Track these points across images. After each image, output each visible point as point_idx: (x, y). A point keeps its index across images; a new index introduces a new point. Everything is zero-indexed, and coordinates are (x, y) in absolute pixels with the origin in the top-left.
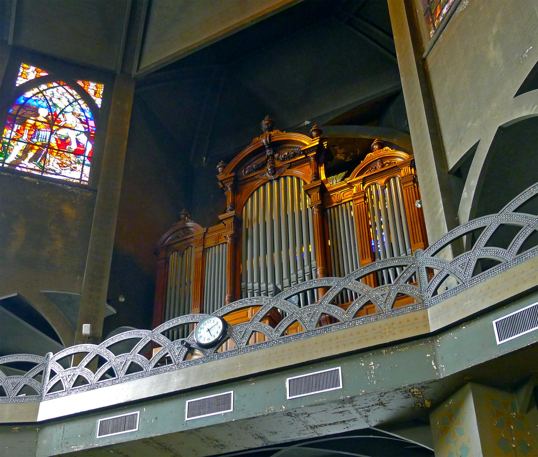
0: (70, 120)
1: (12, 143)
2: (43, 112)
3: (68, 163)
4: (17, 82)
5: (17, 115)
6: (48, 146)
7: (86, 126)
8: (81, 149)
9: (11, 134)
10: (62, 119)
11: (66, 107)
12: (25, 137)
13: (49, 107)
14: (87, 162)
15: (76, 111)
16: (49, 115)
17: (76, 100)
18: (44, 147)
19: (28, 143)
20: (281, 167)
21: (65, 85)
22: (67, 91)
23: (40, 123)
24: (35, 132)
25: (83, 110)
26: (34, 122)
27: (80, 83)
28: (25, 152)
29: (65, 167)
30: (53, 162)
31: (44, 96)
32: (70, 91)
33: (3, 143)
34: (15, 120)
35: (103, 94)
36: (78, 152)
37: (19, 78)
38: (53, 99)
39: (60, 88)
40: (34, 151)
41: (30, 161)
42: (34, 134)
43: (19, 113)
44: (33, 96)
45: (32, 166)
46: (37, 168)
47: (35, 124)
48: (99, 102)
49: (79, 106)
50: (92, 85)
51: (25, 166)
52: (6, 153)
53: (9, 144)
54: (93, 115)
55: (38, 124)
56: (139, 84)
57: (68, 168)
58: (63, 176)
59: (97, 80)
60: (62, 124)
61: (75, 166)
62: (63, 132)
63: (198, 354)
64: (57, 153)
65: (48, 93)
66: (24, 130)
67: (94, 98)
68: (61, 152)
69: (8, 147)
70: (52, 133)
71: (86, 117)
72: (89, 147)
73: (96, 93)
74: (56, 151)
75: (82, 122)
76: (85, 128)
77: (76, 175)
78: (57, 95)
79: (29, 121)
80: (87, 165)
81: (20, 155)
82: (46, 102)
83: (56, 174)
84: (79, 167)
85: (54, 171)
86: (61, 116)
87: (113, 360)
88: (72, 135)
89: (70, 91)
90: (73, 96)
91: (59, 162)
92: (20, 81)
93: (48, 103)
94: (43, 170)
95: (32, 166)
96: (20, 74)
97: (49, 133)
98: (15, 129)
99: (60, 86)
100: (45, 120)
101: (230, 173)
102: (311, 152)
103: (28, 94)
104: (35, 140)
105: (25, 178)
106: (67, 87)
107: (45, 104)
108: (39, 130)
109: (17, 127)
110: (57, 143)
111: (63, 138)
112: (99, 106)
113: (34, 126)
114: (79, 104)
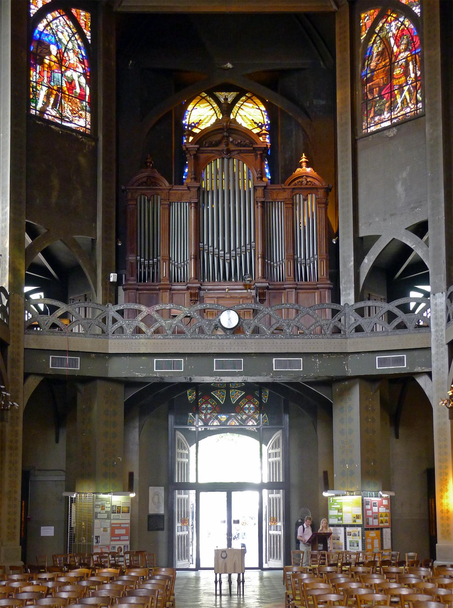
0: (72, 58)
1: (38, 87)
2: (53, 49)
3: (76, 109)
4: (31, 11)
6: (60, 90)
7: (83, 66)
8: (83, 93)
9: (36, 76)
10: (67, 59)
11: (68, 42)
12: (46, 80)
13: (56, 44)
14: (88, 108)
16: (57, 54)
18: (59, 92)
19: (49, 87)
20: (233, 151)
21: (64, 15)
22: (67, 23)
23: (53, 63)
24: (51, 73)
26: (49, 61)
27: (73, 11)
28: (48, 96)
29: (75, 114)
31: (52, 29)
32: (68, 22)
35: (91, 27)
36: (81, 97)
38: (58, 33)
39: (61, 18)
40: (54, 96)
41: (52, 109)
42: (51, 76)
43: (39, 51)
44: (44, 30)
45: (54, 113)
46: (58, 115)
47: (50, 63)
49: (75, 41)
50: (83, 13)
51: (50, 113)
52: (36, 100)
53: (36, 87)
55: (53, 63)
57: (77, 115)
58: (75, 124)
59: (84, 9)
60: (67, 64)
61: (81, 112)
63: (220, 332)
64: (69, 99)
65: (54, 26)
66: (44, 71)
68: (70, 97)
69: (36, 91)
70: (62, 74)
71: (82, 55)
73: (86, 25)
74: (67, 96)
75: (80, 62)
76: (83, 69)
77: (82, 123)
78: (60, 28)
82: (54, 37)
83: (71, 122)
84: (83, 113)
85: (68, 118)
86: (65, 55)
87: (164, 323)
88: (75, 76)
89: (68, 22)
90: (70, 29)
91: (71, 109)
92: (33, 10)
93: (55, 38)
94: (62, 118)
95: (54, 113)
97: (60, 75)
98: (38, 72)
99: (62, 16)
101: (195, 144)
102: (259, 150)
103: (41, 27)
104: (52, 83)
105: (52, 127)
107: (53, 40)
108: (54, 71)
111: (70, 81)
114: (76, 39)
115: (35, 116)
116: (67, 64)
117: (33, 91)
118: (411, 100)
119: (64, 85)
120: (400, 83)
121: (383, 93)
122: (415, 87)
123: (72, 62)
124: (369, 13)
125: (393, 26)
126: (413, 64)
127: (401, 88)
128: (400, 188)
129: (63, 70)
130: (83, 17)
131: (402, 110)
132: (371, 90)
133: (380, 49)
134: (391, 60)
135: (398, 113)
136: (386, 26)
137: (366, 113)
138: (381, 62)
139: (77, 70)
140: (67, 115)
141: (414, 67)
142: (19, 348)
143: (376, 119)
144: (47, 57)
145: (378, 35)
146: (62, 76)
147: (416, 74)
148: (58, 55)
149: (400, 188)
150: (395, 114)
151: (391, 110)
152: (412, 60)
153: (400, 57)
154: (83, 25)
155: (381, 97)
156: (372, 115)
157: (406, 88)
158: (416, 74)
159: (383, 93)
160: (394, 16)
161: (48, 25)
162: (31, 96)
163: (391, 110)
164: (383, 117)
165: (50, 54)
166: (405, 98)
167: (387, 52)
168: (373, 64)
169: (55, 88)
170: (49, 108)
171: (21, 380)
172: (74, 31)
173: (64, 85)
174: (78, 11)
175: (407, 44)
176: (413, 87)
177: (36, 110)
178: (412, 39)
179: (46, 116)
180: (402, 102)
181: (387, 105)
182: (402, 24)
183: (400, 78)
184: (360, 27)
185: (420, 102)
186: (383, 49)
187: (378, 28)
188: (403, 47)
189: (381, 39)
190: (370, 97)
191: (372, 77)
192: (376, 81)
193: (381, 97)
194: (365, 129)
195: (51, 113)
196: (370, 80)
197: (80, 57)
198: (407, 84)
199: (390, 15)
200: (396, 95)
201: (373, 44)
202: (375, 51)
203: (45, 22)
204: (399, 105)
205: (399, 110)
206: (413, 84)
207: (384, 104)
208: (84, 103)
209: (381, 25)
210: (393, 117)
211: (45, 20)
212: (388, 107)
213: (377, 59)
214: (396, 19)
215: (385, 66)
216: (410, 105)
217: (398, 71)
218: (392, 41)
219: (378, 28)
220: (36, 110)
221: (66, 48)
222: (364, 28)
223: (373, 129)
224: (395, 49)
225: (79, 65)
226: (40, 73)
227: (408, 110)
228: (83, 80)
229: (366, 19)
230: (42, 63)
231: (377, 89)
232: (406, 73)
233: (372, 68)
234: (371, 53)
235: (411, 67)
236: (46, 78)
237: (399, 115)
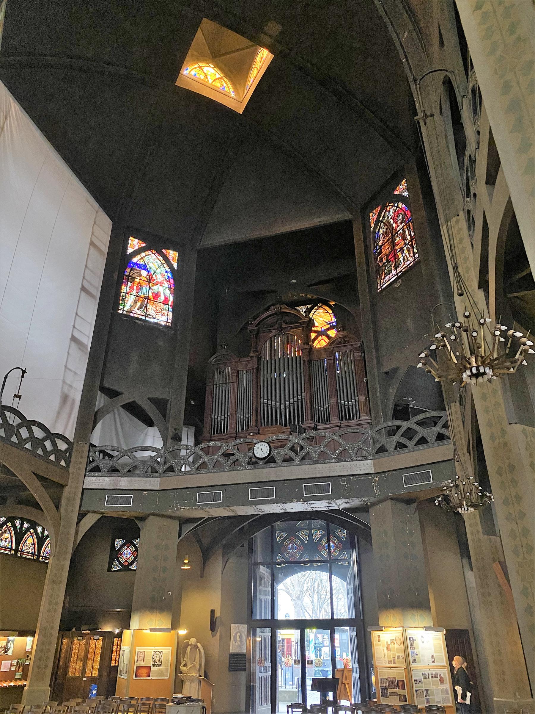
0: (159, 278)
1: (127, 296)
5: (129, 276)
6: (147, 298)
10: (155, 278)
14: (171, 309)
15: (162, 272)
17: (162, 264)
18: (146, 299)
20: (286, 328)
25: (166, 272)
27: (164, 251)
28: (135, 302)
30: (151, 310)
32: (158, 257)
33: (122, 296)
34: (128, 279)
37: (129, 248)
40: (140, 302)
41: (138, 309)
43: (131, 274)
48: (175, 265)
54: (172, 275)
55: (142, 281)
56: (200, 251)
60: (154, 282)
61: (163, 312)
62: (156, 288)
65: (146, 259)
67: (173, 262)
72: (171, 299)
73: (173, 258)
75: (166, 281)
77: (164, 318)
78: (151, 260)
79: (136, 280)
80: (170, 311)
81: (132, 304)
86: (154, 276)
92: (130, 251)
96: (129, 245)
97: (148, 288)
98: (128, 286)
100: (146, 279)
103: (135, 260)
104: (140, 294)
106: (157, 255)
109: (130, 284)
110: (153, 296)
112: (176, 269)
113: (139, 283)
115: (123, 314)
116: (154, 282)
117: (123, 298)
119: (151, 295)
123: (159, 281)
124: (374, 211)
125: (391, 211)
126: (408, 229)
127: (402, 250)
128: (410, 324)
129: (151, 285)
130: (173, 255)
131: (404, 264)
132: (381, 259)
133: (384, 230)
135: (402, 268)
136: (387, 214)
139: (163, 285)
140: (151, 314)
141: (409, 232)
142: (77, 487)
143: (387, 278)
144: (138, 278)
145: (382, 222)
146: (149, 289)
148: (148, 277)
149: (410, 324)
150: (399, 270)
151: (396, 268)
153: (398, 229)
154: (171, 259)
155: (388, 261)
157: (405, 248)
160: (391, 204)
161: (142, 258)
162: (121, 302)
163: (396, 268)
164: (391, 274)
165: (141, 275)
167: (391, 232)
168: (380, 243)
169: (143, 296)
170: (136, 310)
171: (75, 518)
172: (164, 262)
173: (151, 295)
174: (167, 251)
175: (403, 218)
177: (123, 310)
178: (405, 213)
179: (131, 314)
180: (404, 259)
182: (397, 207)
184: (370, 222)
185: (416, 253)
186: (386, 229)
187: (381, 218)
188: (400, 221)
189: (384, 223)
190: (381, 265)
191: (381, 250)
192: (384, 252)
193: (388, 261)
195: (137, 313)
196: (380, 253)
197: (166, 277)
198: (406, 245)
199: (389, 206)
201: (379, 229)
202: (381, 232)
203: (138, 257)
204: (402, 261)
207: (391, 266)
208: (167, 306)
209: (383, 214)
211: (139, 256)
214: (392, 206)
215: (389, 239)
216: (409, 258)
217: (398, 239)
218: (392, 221)
219: (381, 218)
220: (123, 310)
221: (155, 272)
222: (372, 222)
223: (384, 286)
224: (394, 225)
225: (165, 282)
226: (130, 287)
227: (409, 262)
228: (168, 292)
229: (373, 216)
230: (133, 281)
232: (404, 238)
234: (379, 235)
235: (407, 233)
236: (135, 290)
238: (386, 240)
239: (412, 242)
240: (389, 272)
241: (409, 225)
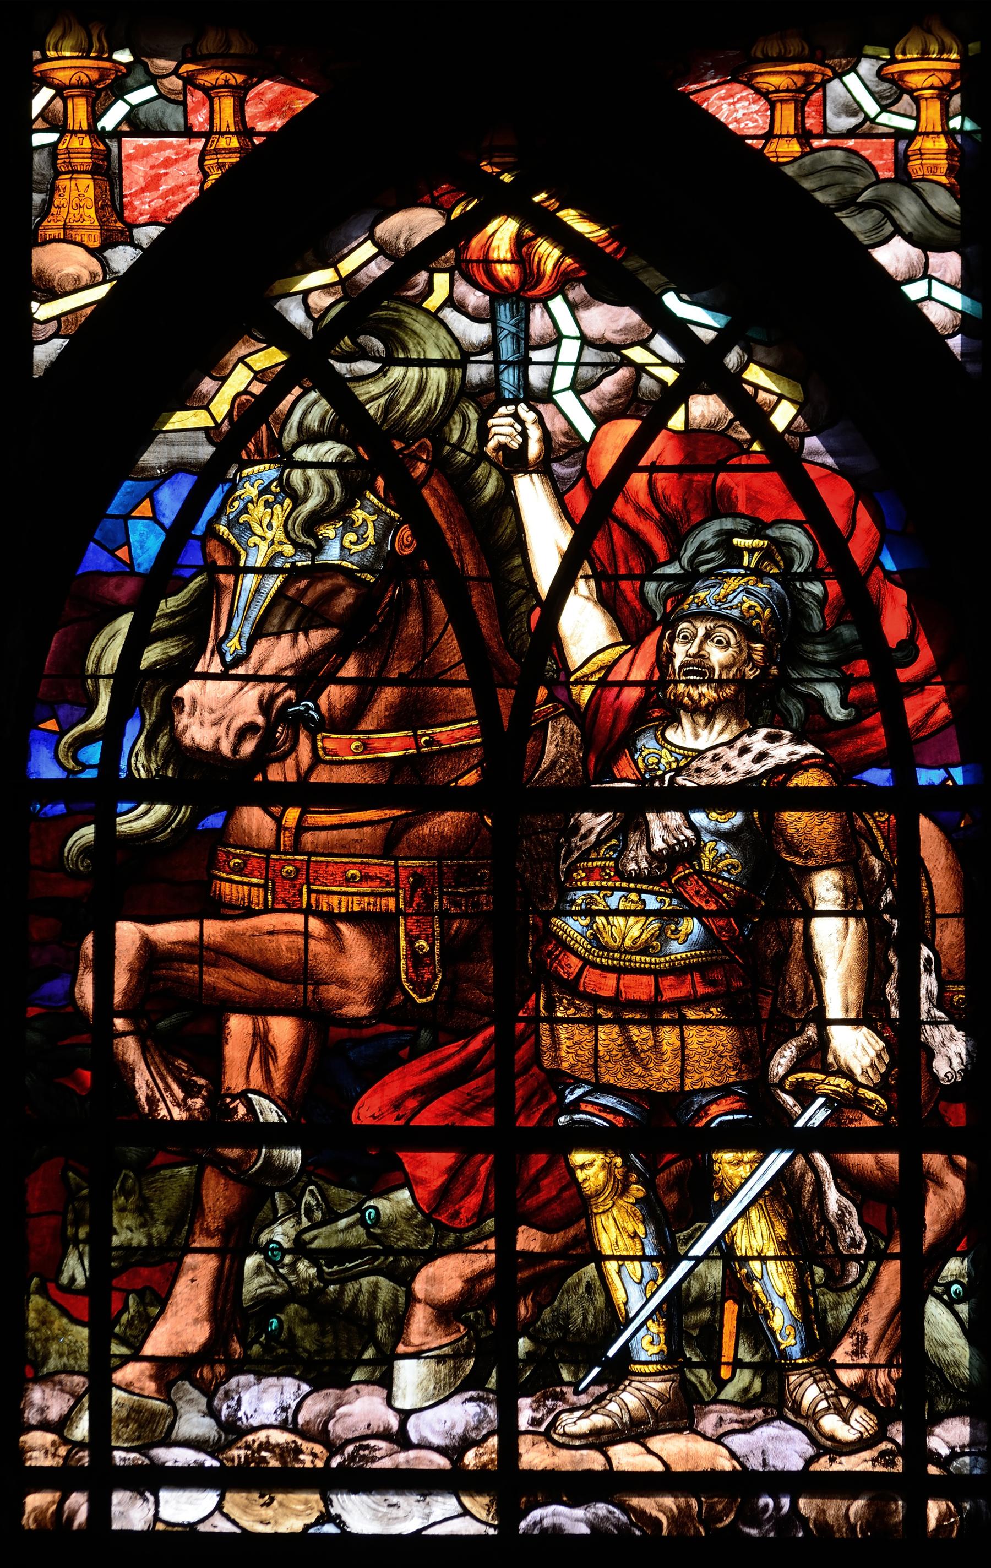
118: (820, 1339)
120: (663, 1077)
121: (369, 1109)
122: (893, 1206)
131: (679, 1413)
134: (507, 744)
137: (75, 1269)
138: (347, 721)
143: (263, 1401)
147: (906, 1049)
152: (848, 859)
156: (182, 1326)
157: (747, 1174)
158: (906, 1049)
159: (369, 1109)
164: (363, 1409)
166: (737, 1286)
168: (215, 710)
176: (848, 1181)
181: (445, 1277)
183: (652, 1012)
194: (61, 1479)
196: (175, 876)
198: (764, 1127)
200: (581, 1208)
204: (647, 1344)
205: (630, 1399)
206: (863, 1160)
210: (534, 1456)
212: (445, 1314)
213: (279, 653)
215: (410, 787)
216: (811, 1394)
227: (783, 1447)
231: (283, 1030)
232: (755, 979)
233: (198, 732)
235: (835, 945)
237: (627, 1457)
238: (346, 758)
239: (915, 1183)
240: (343, 1347)
241: (907, 842)
